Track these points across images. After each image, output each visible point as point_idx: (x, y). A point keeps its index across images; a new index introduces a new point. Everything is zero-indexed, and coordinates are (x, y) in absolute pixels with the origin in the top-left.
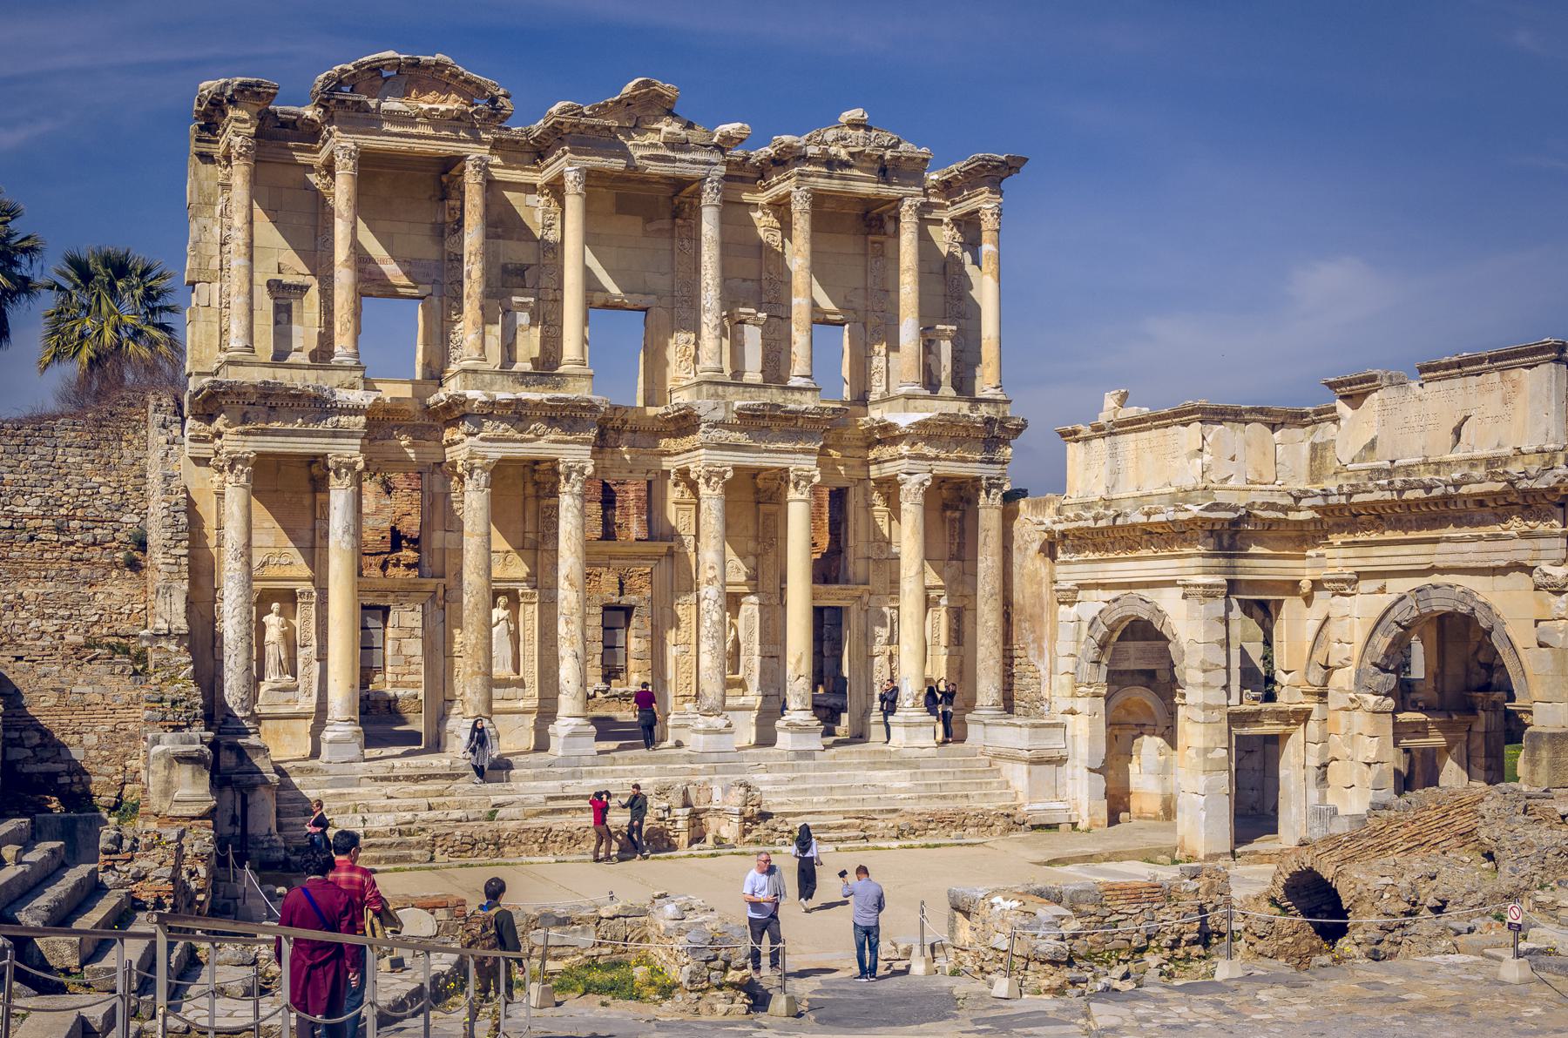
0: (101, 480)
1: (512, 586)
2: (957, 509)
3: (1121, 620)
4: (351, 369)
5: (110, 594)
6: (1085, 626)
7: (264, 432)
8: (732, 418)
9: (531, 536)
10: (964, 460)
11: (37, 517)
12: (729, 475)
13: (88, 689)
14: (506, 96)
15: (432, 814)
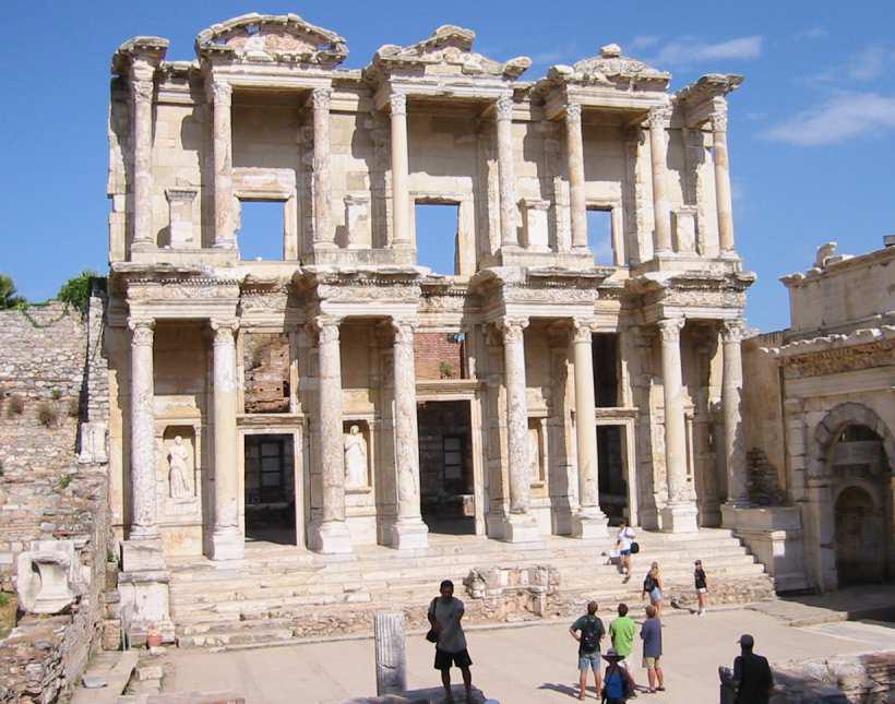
0: (58, 350)
1: (361, 417)
2: (706, 346)
3: (842, 425)
4: (227, 252)
5: (65, 435)
6: (811, 432)
7: (159, 302)
8: (524, 278)
9: (375, 378)
10: (707, 306)
11: (11, 380)
12: (526, 324)
13: (15, 507)
14: (341, 42)
15: (296, 600)
